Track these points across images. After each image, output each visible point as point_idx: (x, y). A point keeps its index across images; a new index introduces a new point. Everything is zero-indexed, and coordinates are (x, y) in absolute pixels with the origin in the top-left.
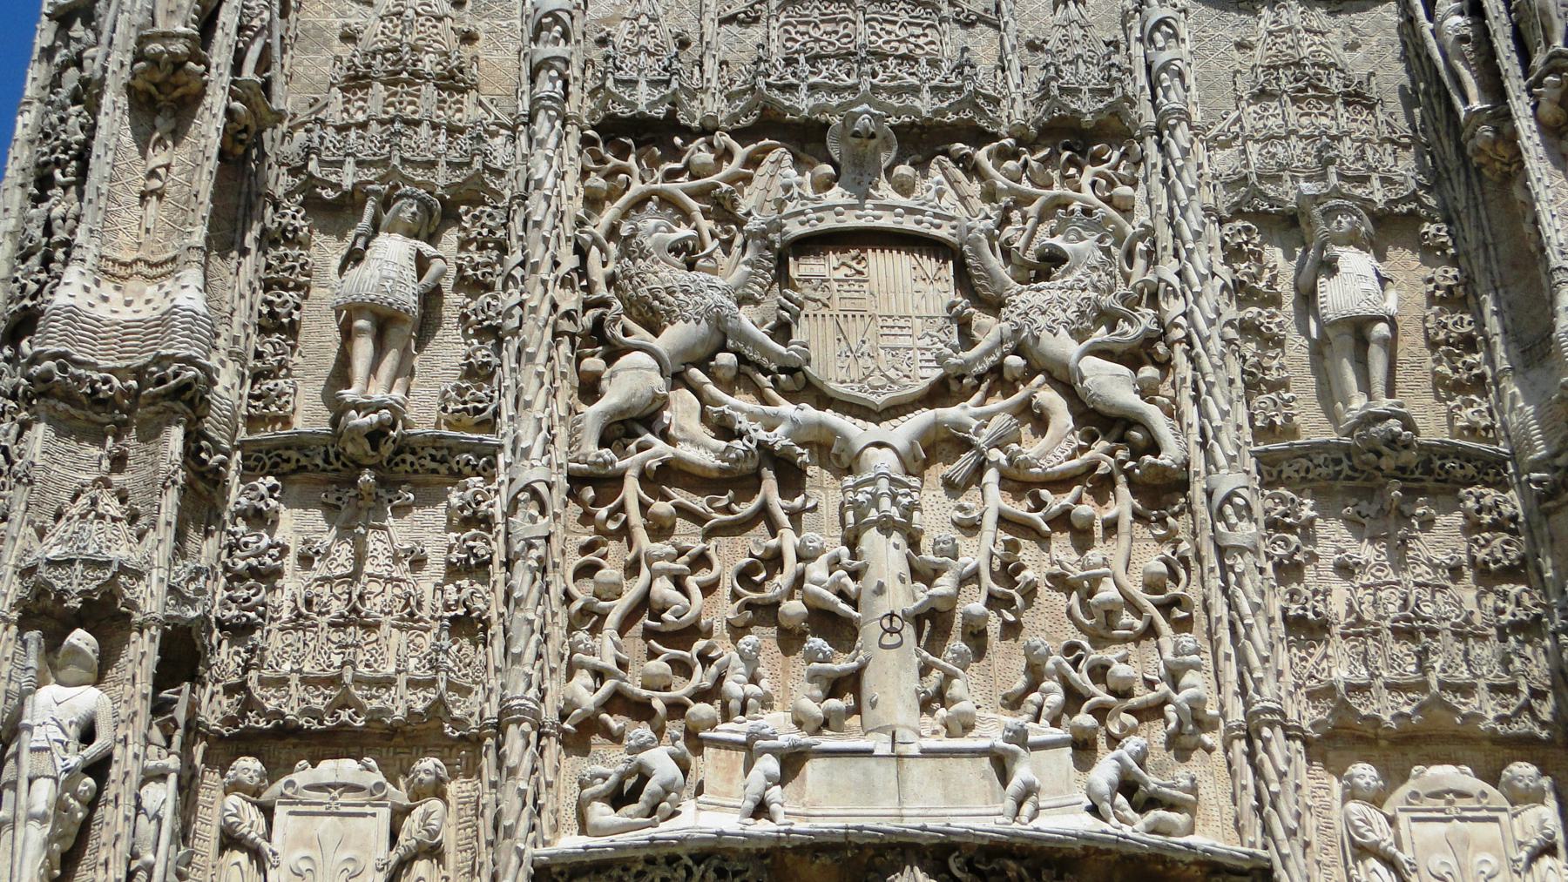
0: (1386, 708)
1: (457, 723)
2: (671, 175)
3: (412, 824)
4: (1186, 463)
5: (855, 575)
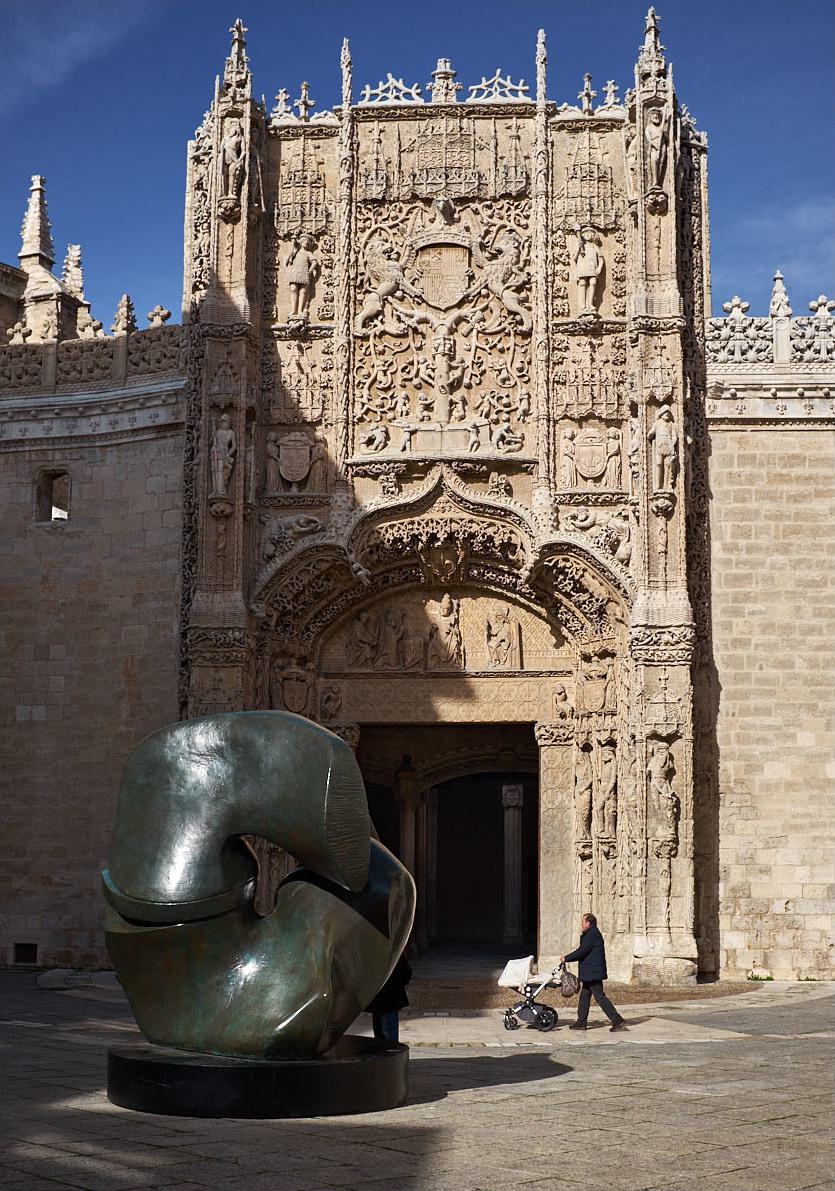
0: (575, 412)
1: (326, 420)
2: (384, 220)
3: (315, 450)
4: (532, 329)
5: (433, 370)
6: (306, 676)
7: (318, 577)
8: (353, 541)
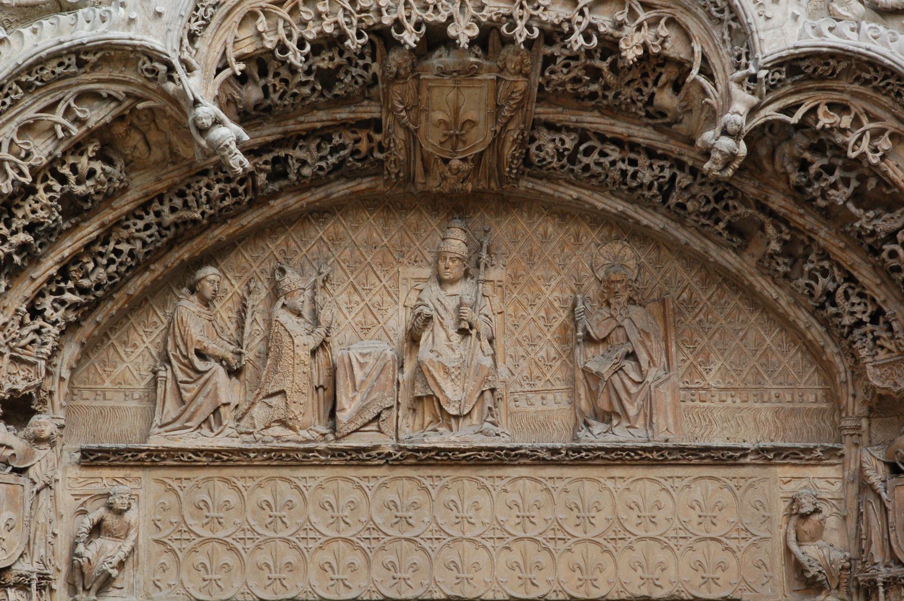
6: (28, 456)
7: (78, 148)
8: (192, 37)
